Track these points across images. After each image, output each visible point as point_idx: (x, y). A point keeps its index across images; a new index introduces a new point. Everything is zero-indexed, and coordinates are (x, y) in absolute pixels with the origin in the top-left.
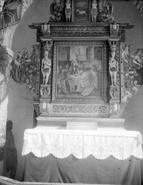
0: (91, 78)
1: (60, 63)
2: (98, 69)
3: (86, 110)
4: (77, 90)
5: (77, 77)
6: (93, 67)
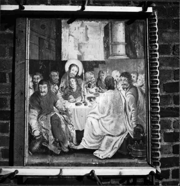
0: (117, 108)
2: (134, 84)
4: (83, 145)
5: (82, 106)
6: (123, 78)
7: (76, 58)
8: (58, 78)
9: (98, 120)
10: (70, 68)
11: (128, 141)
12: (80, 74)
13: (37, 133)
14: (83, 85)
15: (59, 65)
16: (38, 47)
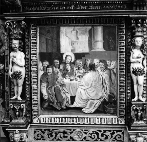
1: (43, 57)
3: (91, 137)
4: (75, 105)
5: (75, 81)
6: (101, 64)
7: (70, 51)
8: (58, 63)
9: (85, 90)
10: (66, 57)
11: (104, 103)
12: (72, 61)
13: (46, 98)
14: (75, 69)
15: (60, 56)
16: (45, 44)
